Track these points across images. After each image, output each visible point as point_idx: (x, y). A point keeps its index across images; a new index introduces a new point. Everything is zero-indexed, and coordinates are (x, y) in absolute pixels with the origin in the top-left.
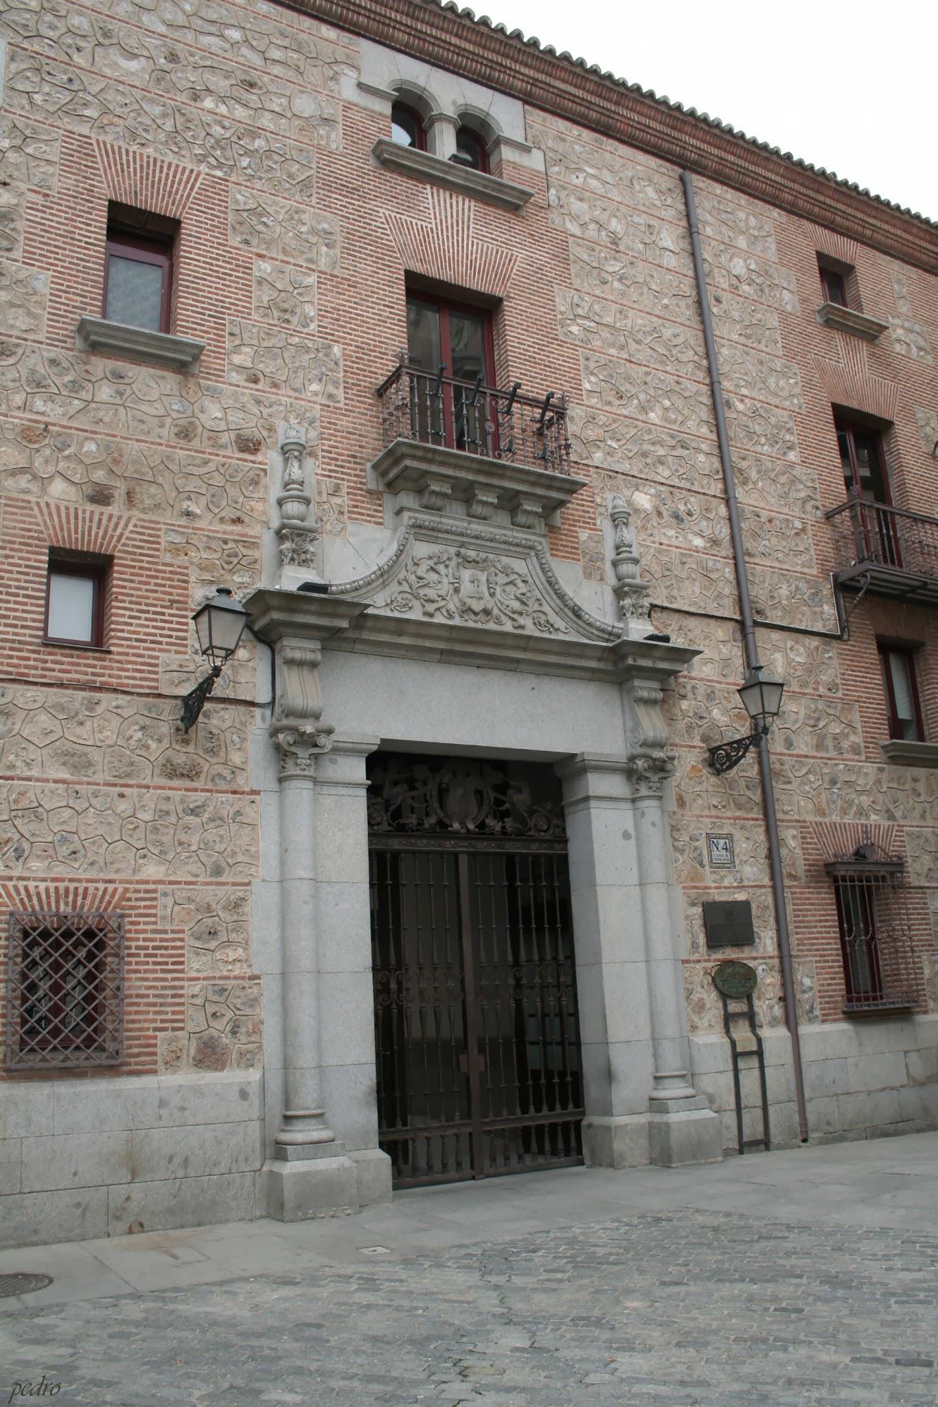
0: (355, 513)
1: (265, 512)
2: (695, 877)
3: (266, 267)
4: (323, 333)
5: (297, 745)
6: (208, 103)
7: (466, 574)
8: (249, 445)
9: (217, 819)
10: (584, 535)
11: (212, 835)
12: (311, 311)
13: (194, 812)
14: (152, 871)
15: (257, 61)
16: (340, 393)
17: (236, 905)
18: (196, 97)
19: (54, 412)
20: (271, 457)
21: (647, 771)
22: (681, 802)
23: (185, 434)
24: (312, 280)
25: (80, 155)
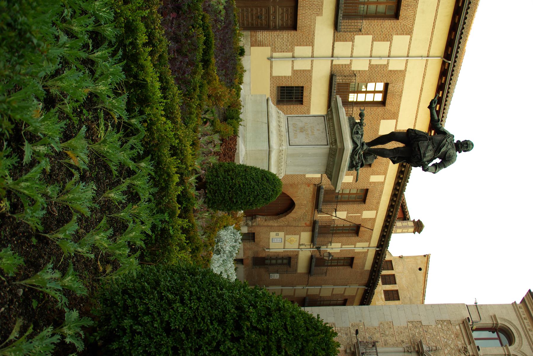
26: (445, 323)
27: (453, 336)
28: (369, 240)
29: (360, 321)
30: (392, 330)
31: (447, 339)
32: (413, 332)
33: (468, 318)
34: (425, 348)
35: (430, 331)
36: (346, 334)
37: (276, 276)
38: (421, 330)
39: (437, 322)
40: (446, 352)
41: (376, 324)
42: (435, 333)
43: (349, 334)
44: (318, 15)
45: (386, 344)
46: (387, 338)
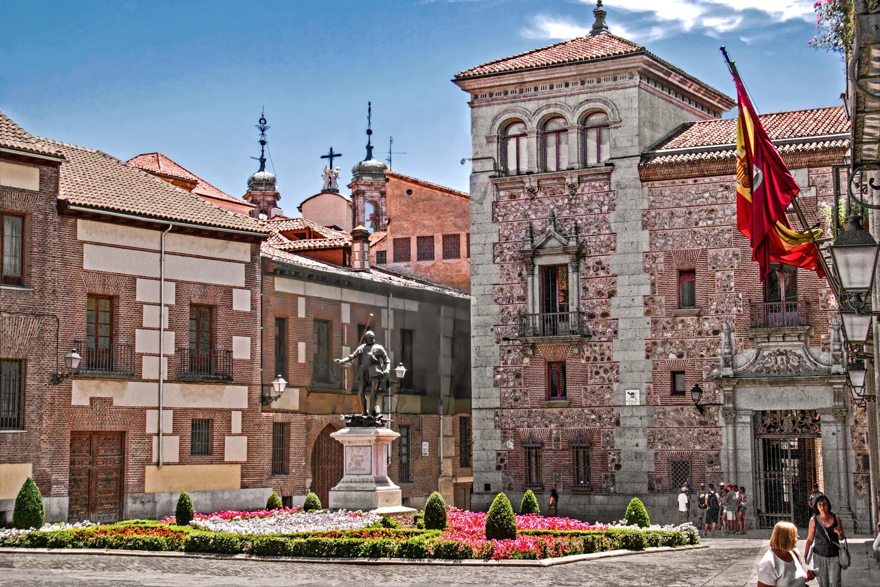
0: (745, 347)
1: (722, 350)
2: (860, 447)
3: (719, 274)
4: (736, 291)
5: (733, 415)
6: (701, 224)
7: (779, 358)
8: (716, 332)
9: (712, 434)
10: (823, 337)
11: (711, 438)
12: (732, 284)
13: (707, 433)
14: (698, 447)
15: (714, 200)
16: (741, 309)
17: (717, 456)
18: (697, 224)
19: (669, 335)
20: (722, 335)
21: (842, 415)
22: (856, 422)
23: (700, 333)
24: (732, 274)
25: (669, 257)
26: (497, 210)
27: (514, 203)
28: (377, 310)
29: (492, 330)
30: (504, 287)
31: (518, 210)
32: (508, 258)
33: (490, 177)
34: (528, 247)
35: (506, 233)
36: (509, 352)
37: (425, 446)
38: (504, 246)
39: (495, 220)
40: (533, 216)
41: (496, 309)
42: (509, 227)
43: (509, 348)
44: (112, 403)
45: (523, 299)
46: (515, 295)
